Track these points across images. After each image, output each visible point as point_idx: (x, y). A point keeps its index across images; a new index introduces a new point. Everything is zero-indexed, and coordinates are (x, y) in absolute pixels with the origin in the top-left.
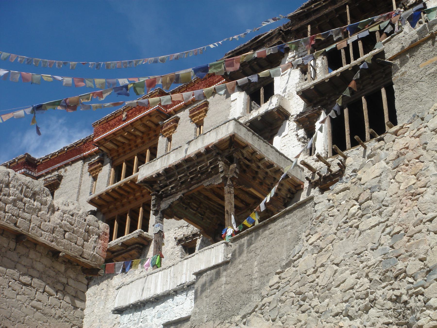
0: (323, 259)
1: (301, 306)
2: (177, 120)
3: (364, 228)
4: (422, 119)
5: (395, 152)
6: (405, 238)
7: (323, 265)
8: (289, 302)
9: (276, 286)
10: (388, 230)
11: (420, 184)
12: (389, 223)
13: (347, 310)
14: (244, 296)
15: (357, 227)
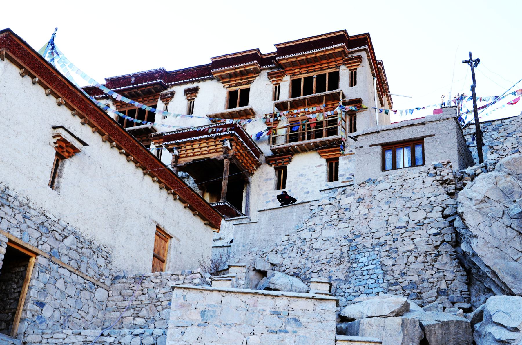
0: (315, 235)
2: (173, 94)
3: (341, 227)
6: (361, 238)
10: (352, 231)
11: (370, 214)
12: (354, 228)
13: (329, 262)
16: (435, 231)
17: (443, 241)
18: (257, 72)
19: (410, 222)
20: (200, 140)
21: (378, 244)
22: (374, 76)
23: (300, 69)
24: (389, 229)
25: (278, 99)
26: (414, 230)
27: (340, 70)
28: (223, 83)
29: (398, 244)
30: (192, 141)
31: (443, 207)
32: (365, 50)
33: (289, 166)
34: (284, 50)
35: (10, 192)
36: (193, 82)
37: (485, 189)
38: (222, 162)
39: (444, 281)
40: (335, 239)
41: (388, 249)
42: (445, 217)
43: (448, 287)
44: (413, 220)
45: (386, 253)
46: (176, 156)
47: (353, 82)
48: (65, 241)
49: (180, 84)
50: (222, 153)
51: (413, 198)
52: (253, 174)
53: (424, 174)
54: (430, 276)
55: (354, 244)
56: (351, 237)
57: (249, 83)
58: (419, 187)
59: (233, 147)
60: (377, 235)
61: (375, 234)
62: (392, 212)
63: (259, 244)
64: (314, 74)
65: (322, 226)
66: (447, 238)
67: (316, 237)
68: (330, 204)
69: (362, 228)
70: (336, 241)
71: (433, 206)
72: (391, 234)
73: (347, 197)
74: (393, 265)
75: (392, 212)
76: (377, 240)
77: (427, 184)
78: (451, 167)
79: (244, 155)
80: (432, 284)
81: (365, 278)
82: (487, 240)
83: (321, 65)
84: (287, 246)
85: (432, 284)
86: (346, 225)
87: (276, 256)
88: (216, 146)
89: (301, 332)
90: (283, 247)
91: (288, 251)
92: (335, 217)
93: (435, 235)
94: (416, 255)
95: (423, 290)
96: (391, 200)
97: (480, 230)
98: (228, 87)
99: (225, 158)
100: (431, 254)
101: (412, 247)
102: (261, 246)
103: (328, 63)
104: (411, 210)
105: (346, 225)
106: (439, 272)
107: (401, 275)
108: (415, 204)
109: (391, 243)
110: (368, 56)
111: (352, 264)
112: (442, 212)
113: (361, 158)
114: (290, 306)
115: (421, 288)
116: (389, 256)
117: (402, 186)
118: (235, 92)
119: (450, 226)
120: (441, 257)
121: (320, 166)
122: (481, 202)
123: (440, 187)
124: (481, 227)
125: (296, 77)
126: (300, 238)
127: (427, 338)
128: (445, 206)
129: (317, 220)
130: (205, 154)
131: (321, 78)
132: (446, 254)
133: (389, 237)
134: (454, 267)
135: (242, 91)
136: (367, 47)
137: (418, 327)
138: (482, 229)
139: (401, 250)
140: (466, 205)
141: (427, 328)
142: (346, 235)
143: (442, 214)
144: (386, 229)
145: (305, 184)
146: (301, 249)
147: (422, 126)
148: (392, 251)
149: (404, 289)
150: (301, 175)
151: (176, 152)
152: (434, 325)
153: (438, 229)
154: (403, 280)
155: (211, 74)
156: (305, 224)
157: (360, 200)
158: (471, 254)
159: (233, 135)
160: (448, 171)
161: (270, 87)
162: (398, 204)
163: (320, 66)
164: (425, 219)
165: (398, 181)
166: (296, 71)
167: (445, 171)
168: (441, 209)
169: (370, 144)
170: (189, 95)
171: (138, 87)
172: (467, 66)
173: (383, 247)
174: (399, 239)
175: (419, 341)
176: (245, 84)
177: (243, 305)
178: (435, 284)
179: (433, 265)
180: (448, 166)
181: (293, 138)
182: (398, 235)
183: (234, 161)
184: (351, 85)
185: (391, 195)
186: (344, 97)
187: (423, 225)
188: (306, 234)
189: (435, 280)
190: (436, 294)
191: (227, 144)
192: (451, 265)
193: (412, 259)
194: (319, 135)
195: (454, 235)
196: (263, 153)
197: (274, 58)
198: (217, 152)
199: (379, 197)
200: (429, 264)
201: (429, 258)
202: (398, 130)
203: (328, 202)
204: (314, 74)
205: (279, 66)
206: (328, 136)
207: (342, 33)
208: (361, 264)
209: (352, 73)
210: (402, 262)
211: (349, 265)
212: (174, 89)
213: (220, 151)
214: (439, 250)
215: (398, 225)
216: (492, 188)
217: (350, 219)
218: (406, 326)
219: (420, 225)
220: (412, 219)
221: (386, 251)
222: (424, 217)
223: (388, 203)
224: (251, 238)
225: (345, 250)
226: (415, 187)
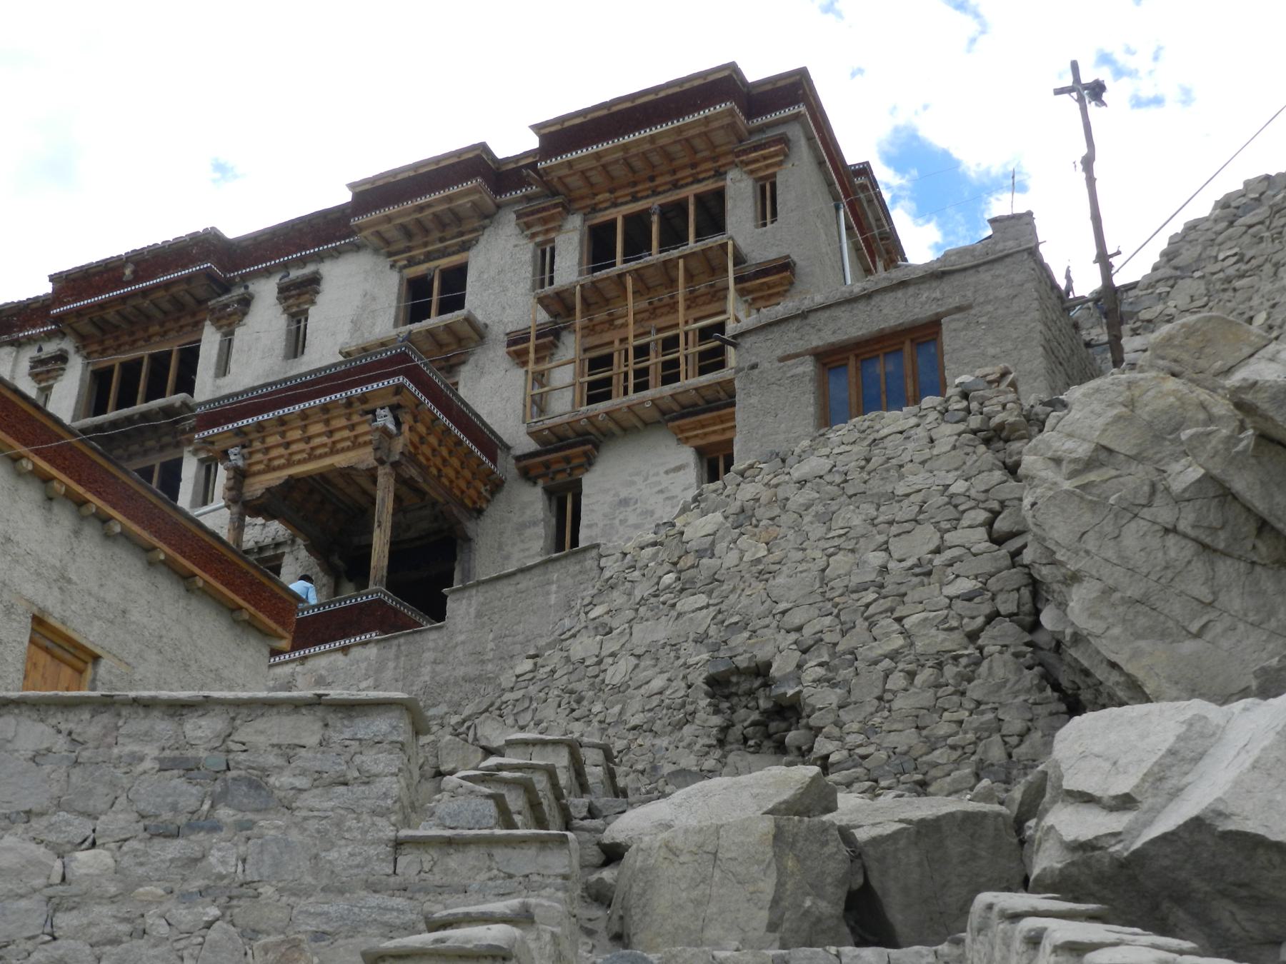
0: (612, 645)
1: (573, 710)
2: (246, 302)
3: (686, 608)
4: (783, 461)
5: (738, 503)
6: (746, 634)
7: (613, 655)
8: (553, 701)
9: (531, 675)
10: (720, 617)
11: (772, 558)
12: (723, 607)
13: (652, 721)
14: (467, 687)
15: (674, 605)
16: (965, 585)
17: (990, 619)
19: (892, 565)
20: (304, 415)
22: (836, 198)
23: (611, 191)
24: (828, 595)
25: (551, 283)
26: (903, 589)
27: (728, 182)
28: (390, 255)
30: (282, 421)
31: (991, 511)
33: (590, 482)
34: (561, 136)
36: (303, 262)
37: (1100, 422)
38: (372, 475)
39: (996, 738)
40: (668, 648)
41: (826, 658)
42: (998, 540)
43: (1010, 756)
44: (900, 561)
49: (268, 273)
50: (370, 449)
51: (901, 490)
52: (480, 512)
53: (933, 416)
54: (954, 727)
57: (465, 247)
58: (918, 458)
59: (405, 428)
60: (796, 618)
62: (836, 542)
63: (449, 695)
64: (654, 203)
65: (630, 614)
66: (1007, 604)
67: (615, 648)
68: (654, 544)
70: (672, 654)
71: (961, 508)
72: (836, 611)
73: (704, 513)
75: (836, 542)
76: (793, 636)
77: (943, 446)
78: (1013, 384)
80: (959, 752)
82: (1111, 582)
84: (533, 689)
85: (959, 752)
86: (702, 600)
88: (352, 427)
89: (271, 825)
90: (519, 694)
91: (535, 705)
92: (669, 579)
93: (969, 597)
94: (910, 667)
95: (933, 773)
97: (1087, 552)
98: (405, 267)
99: (381, 461)
100: (956, 659)
101: (899, 642)
102: (456, 698)
103: (694, 166)
104: (895, 529)
105: (702, 600)
106: (983, 713)
108: (906, 511)
110: (810, 139)
112: (989, 524)
113: (754, 400)
114: (236, 737)
115: (925, 768)
116: (828, 681)
117: (868, 460)
119: (1014, 567)
120: (985, 663)
121: (678, 469)
122: (1090, 464)
123: (982, 448)
124: (1091, 543)
126: (568, 659)
127: (875, 883)
128: (996, 506)
129: (618, 598)
130: (321, 456)
132: (1001, 653)
133: (828, 620)
134: (1028, 691)
137: (835, 847)
138: (1094, 550)
140: (1044, 480)
142: (701, 631)
144: (820, 599)
145: (637, 527)
146: (572, 692)
148: (836, 661)
150: (624, 502)
153: (976, 577)
154: (871, 749)
155: (351, 233)
156: (582, 615)
157: (744, 518)
158: (1068, 638)
159: (399, 389)
160: (1002, 399)
161: (525, 252)
162: (854, 516)
163: (668, 178)
164: (937, 551)
165: (855, 448)
166: (600, 197)
167: (994, 401)
168: (982, 516)
169: (779, 352)
170: (291, 301)
171: (145, 293)
172: (1069, 101)
175: (842, 894)
176: (454, 253)
177: (61, 743)
178: (969, 749)
179: (963, 694)
180: (1003, 386)
181: (598, 391)
183: (413, 472)
185: (833, 490)
186: (739, 260)
187: (929, 574)
188: (583, 647)
189: (970, 736)
191: (385, 419)
192: (1017, 687)
193: (897, 681)
195: (1026, 592)
196: (508, 448)
197: (533, 166)
200: (950, 689)
201: (950, 671)
202: (861, 306)
203: (650, 537)
207: (726, 73)
210: (866, 689)
213: (366, 444)
215: (855, 580)
216: (1118, 418)
219: (924, 572)
220: (896, 556)
221: (821, 665)
222: (932, 546)
223: (826, 519)
224: (427, 678)
226: (906, 457)
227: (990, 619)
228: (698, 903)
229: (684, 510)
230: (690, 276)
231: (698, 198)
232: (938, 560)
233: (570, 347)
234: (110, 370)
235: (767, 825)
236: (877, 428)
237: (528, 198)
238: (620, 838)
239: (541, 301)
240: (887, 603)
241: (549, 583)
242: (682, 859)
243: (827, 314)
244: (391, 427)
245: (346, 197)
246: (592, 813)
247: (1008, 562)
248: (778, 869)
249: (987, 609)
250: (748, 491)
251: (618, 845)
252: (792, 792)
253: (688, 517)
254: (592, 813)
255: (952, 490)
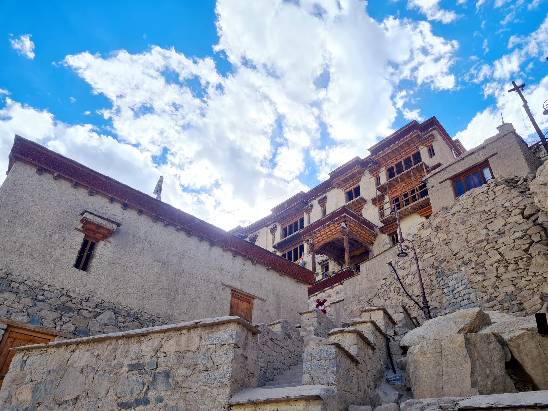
2: (312, 206)
3: (426, 258)
6: (446, 263)
12: (437, 255)
16: (519, 234)
17: (531, 244)
18: (361, 173)
20: (324, 228)
21: (463, 263)
22: (451, 148)
24: (470, 246)
26: (496, 240)
29: (483, 258)
31: (521, 209)
32: (435, 129)
34: (375, 150)
35: (13, 278)
36: (322, 194)
45: (473, 271)
46: (311, 244)
47: (432, 153)
48: (98, 318)
49: (315, 198)
52: (373, 243)
54: (528, 283)
55: (440, 270)
56: (436, 265)
57: (358, 182)
61: (458, 255)
62: (469, 229)
65: (409, 262)
67: (407, 273)
69: (444, 253)
71: (510, 210)
73: (426, 229)
74: (483, 281)
75: (469, 229)
79: (360, 230)
80: (532, 291)
81: (458, 300)
83: (405, 151)
87: (378, 299)
90: (383, 290)
93: (521, 238)
96: (466, 219)
100: (521, 259)
101: (499, 257)
102: (367, 294)
104: (488, 222)
105: (430, 254)
106: (537, 276)
107: (494, 289)
108: (491, 215)
109: (476, 259)
111: (443, 291)
113: (435, 196)
115: (520, 298)
116: (477, 273)
117: (474, 203)
118: (351, 191)
120: (534, 259)
125: (389, 167)
127: (517, 358)
131: (408, 161)
132: (539, 254)
135: (355, 189)
136: (436, 126)
139: (487, 263)
140: (542, 192)
141: (511, 343)
142: (431, 264)
143: (523, 216)
144: (467, 247)
147: (483, 150)
149: (501, 303)
151: (311, 241)
152: (521, 336)
153: (522, 231)
154: (498, 294)
157: (438, 228)
159: (345, 217)
161: (373, 179)
162: (474, 221)
164: (505, 225)
165: (469, 200)
168: (519, 211)
171: (290, 209)
173: (468, 266)
174: (483, 252)
175: (503, 365)
179: (528, 269)
182: (481, 249)
184: (431, 156)
185: (465, 214)
186: (427, 167)
187: (504, 233)
189: (535, 285)
190: (540, 301)
193: (502, 270)
194: (414, 199)
195: (543, 233)
197: (370, 159)
198: (337, 233)
199: (453, 220)
201: (521, 264)
204: (402, 160)
205: (376, 163)
206: (422, 197)
208: (451, 287)
209: (429, 149)
210: (492, 275)
211: (441, 291)
212: (312, 202)
214: (529, 252)
215: (478, 239)
217: (432, 248)
218: (475, 345)
219: (501, 233)
221: (472, 268)
222: (503, 224)
223: (463, 223)
225: (433, 278)
227: (531, 244)
228: (438, 375)
229: (420, 230)
230: (414, 174)
231: (413, 155)
232: (506, 228)
233: (387, 198)
234: (286, 228)
235: (461, 338)
236: (474, 192)
237: (370, 167)
238: (406, 344)
239: (378, 189)
240: (491, 245)
241: (386, 257)
242: (428, 356)
243: (451, 167)
244: (345, 226)
245: (329, 177)
246: (396, 334)
247: (533, 224)
248: (471, 358)
249: (529, 241)
250: (437, 220)
251: (406, 347)
252: (470, 319)
253: (421, 231)
254: (396, 334)
255: (505, 206)
